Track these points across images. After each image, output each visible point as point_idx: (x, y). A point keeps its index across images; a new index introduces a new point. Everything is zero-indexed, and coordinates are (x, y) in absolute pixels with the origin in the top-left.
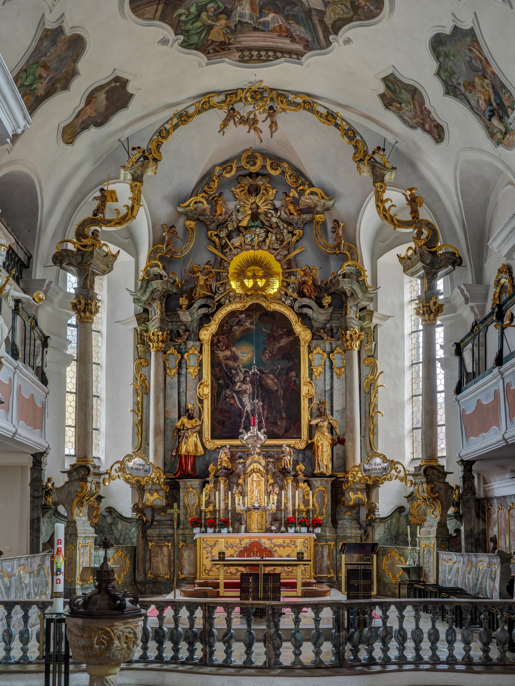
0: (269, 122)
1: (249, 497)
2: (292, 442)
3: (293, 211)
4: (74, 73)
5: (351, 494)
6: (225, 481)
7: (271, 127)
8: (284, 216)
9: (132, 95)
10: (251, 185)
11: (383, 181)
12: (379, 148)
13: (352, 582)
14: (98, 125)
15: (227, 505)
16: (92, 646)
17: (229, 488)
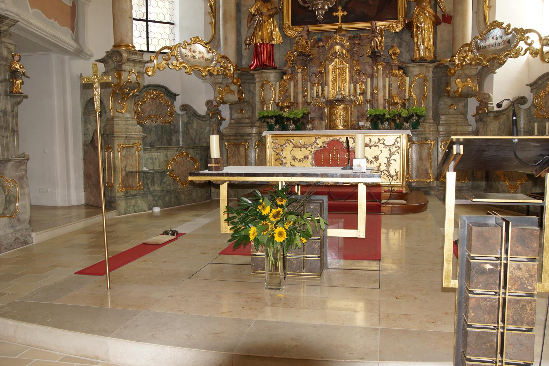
6: (303, 70)
17: (308, 78)
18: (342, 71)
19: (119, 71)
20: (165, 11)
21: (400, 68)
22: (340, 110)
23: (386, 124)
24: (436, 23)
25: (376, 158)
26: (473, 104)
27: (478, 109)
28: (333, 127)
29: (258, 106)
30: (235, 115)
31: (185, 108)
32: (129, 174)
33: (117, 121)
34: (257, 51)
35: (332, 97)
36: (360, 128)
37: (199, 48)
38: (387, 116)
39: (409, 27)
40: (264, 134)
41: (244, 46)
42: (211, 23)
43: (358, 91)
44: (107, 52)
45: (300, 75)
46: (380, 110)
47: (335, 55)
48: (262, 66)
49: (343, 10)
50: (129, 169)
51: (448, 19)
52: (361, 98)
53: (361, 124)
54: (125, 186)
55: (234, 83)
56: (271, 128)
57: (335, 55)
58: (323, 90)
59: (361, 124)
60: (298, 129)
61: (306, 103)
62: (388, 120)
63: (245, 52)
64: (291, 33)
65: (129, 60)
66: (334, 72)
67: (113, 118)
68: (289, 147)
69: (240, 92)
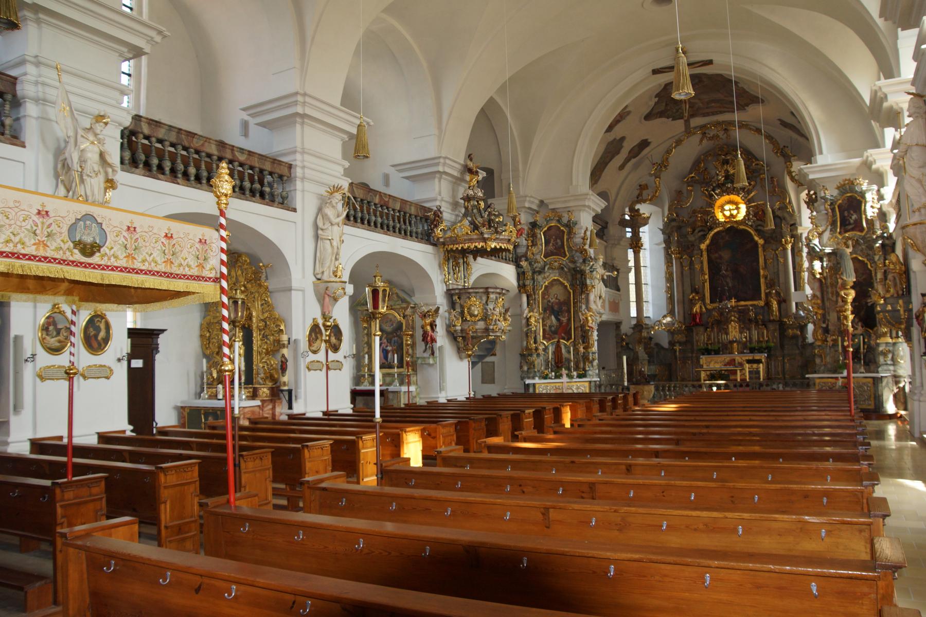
0: (725, 135)
2: (755, 303)
4: (622, 147)
5: (790, 330)
7: (727, 137)
11: (790, 162)
12: (784, 147)
13: (757, 375)
14: (634, 157)
18: (735, 328)
19: (640, 331)
21: (762, 325)
24: (779, 303)
26: (800, 340)
27: (802, 342)
29: (695, 343)
31: (657, 345)
34: (694, 316)
35: (731, 339)
36: (744, 353)
37: (669, 319)
39: (768, 304)
42: (669, 303)
43: (743, 337)
45: (715, 330)
46: (753, 345)
47: (732, 321)
48: (697, 325)
51: (785, 301)
52: (744, 339)
53: (745, 351)
56: (703, 354)
57: (732, 321)
59: (745, 351)
60: (715, 354)
61: (719, 342)
62: (757, 350)
64: (709, 307)
66: (732, 328)
67: (637, 352)
68: (713, 363)
69: (686, 337)
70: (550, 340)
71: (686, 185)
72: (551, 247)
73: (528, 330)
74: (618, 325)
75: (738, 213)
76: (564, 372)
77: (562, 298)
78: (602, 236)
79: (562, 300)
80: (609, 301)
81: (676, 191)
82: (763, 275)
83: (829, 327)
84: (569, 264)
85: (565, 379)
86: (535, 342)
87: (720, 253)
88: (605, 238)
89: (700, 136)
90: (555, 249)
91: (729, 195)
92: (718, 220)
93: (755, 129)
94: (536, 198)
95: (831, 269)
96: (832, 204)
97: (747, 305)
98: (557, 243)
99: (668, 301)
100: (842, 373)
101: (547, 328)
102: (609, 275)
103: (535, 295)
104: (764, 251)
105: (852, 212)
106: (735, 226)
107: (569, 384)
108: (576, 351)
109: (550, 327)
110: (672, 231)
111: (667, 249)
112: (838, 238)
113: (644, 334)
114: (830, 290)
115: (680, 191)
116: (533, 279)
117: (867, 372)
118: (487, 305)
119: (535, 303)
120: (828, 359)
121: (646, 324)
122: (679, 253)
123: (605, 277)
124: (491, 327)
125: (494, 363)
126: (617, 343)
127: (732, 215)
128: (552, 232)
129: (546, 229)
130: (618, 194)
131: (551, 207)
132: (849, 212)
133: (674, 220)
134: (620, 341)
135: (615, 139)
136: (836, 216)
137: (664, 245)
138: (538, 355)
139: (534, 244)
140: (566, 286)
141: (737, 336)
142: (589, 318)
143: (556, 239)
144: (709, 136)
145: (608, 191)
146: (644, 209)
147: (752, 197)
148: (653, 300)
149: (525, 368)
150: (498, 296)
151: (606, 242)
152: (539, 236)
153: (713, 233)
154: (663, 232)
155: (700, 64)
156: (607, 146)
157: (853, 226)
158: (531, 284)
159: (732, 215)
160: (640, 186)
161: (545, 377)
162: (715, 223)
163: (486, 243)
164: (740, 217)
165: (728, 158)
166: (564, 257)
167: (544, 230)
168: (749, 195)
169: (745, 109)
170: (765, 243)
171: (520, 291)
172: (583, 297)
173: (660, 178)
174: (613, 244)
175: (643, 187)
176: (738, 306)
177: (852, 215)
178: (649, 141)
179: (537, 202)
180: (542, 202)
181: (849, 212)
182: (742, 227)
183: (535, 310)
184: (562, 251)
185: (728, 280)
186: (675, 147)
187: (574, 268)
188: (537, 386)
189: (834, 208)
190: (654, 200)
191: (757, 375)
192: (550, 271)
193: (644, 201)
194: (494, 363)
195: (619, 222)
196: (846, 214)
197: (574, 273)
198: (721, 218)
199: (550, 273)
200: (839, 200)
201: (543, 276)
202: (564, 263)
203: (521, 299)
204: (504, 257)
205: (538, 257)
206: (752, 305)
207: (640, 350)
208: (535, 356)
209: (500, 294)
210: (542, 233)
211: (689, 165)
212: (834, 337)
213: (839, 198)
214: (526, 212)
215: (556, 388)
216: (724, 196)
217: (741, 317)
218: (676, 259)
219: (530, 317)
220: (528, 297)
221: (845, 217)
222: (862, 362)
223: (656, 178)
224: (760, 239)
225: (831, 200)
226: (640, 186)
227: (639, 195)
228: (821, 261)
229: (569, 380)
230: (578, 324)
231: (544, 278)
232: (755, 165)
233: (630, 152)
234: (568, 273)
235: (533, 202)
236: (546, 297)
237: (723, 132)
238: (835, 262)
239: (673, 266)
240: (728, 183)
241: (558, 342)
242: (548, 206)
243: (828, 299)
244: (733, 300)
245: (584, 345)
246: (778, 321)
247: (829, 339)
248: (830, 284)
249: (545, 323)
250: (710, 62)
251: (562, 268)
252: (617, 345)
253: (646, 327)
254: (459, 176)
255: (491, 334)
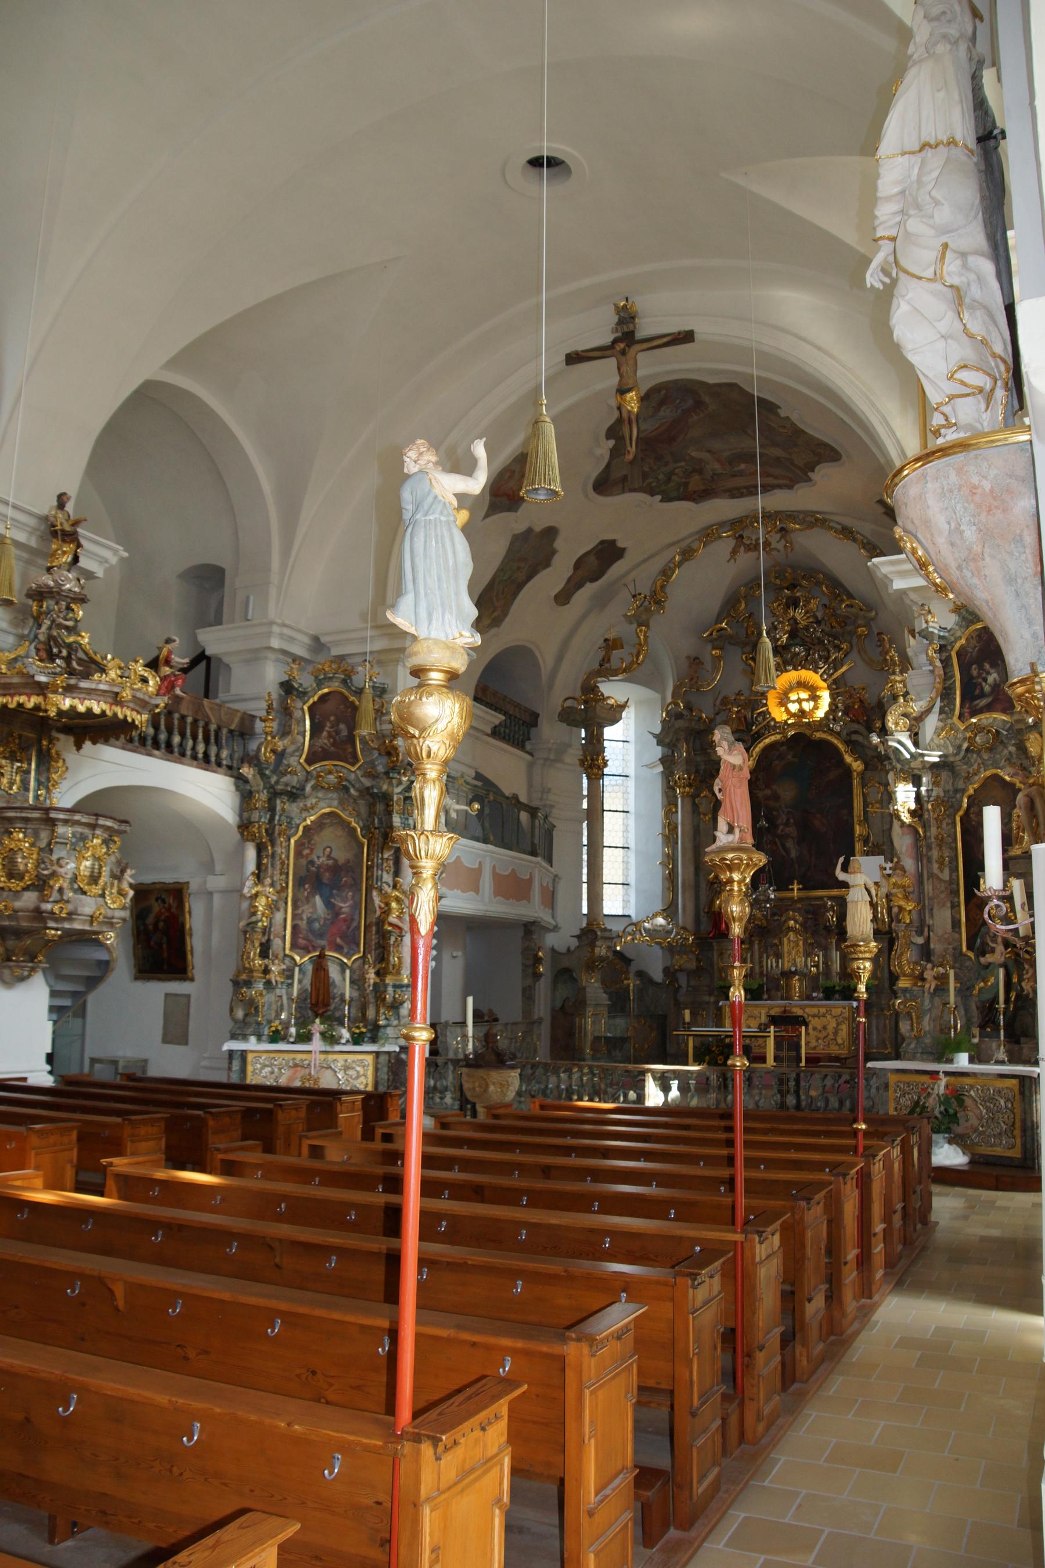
0: (783, 542)
1: (786, 959)
3: (834, 624)
4: (554, 552)
6: (760, 941)
8: (827, 629)
9: (624, 550)
10: (788, 598)
14: (593, 580)
15: (761, 967)
16: (474, 1089)
19: (592, 945)
20: (620, 872)
22: (795, 981)
23: (837, 996)
25: (825, 1028)
28: (788, 998)
30: (693, 983)
31: (641, 974)
32: (597, 1039)
33: (588, 990)
36: (813, 999)
37: (660, 921)
38: (837, 988)
40: (721, 1004)
41: (702, 914)
42: (669, 889)
44: (582, 930)
45: (756, 947)
46: (829, 984)
47: (790, 929)
49: (798, 884)
50: (597, 1034)
53: (814, 995)
54: (592, 1049)
55: (691, 952)
58: (777, 962)
59: (814, 995)
61: (761, 973)
63: (704, 919)
65: (602, 938)
67: (584, 988)
69: (698, 960)
70: (309, 952)
71: (709, 647)
72: (324, 740)
73: (248, 924)
74: (530, 929)
75: (816, 708)
76: (317, 1026)
77: (341, 855)
78: (523, 742)
79: (341, 861)
80: (495, 875)
81: (688, 657)
82: (860, 835)
83: (932, 946)
84: (362, 779)
85: (317, 1044)
86: (264, 954)
87: (774, 787)
88: (528, 746)
89: (732, 543)
90: (334, 744)
91: (796, 669)
92: (774, 719)
93: (839, 527)
94: (300, 631)
95: (939, 802)
96: (942, 649)
97: (821, 898)
98: (338, 732)
99: (667, 885)
100: (950, 1061)
101: (303, 924)
102: (466, 811)
103: (273, 845)
104: (864, 785)
105: (987, 666)
106: (808, 732)
107: (323, 1057)
108: (358, 982)
109: (310, 921)
110: (678, 740)
111: (668, 774)
112: (957, 730)
113: (601, 950)
114: (935, 854)
115: (696, 658)
116: (272, 810)
117: (1013, 1060)
118: (51, 851)
119: (273, 865)
120: (926, 1024)
121: (605, 930)
122: (690, 785)
123: (454, 815)
124: (47, 907)
125: (188, 996)
126: (525, 966)
127: (802, 711)
128: (330, 706)
129: (316, 698)
130: (560, 658)
131: (335, 652)
132: (981, 667)
133: (679, 716)
134: (531, 962)
135: (530, 530)
136: (953, 676)
137: (660, 769)
138: (268, 984)
139: (285, 732)
140: (354, 830)
141: (800, 961)
142: (394, 905)
143: (338, 725)
144: (748, 542)
145: (533, 648)
146: (613, 690)
147: (843, 673)
148: (637, 880)
149: (240, 1014)
150: (87, 831)
151: (531, 754)
152: (297, 714)
153: (761, 745)
154: (660, 740)
155: (665, 340)
156: (512, 543)
157: (990, 699)
158: (265, 819)
159: (802, 711)
160: (606, 640)
161: (276, 1037)
162: (767, 727)
163: (45, 697)
164: (820, 714)
165: (798, 594)
166: (353, 764)
167: (311, 701)
168: (836, 670)
169: (810, 480)
170: (866, 769)
171: (242, 834)
172: (386, 856)
173: (648, 626)
174: (546, 759)
175: (611, 645)
176: (809, 898)
177: (988, 673)
178: (620, 544)
179: (306, 640)
180: (316, 639)
181: (981, 667)
182: (819, 735)
183: (268, 881)
184: (350, 750)
185: (790, 844)
186: (680, 565)
187: (368, 788)
188: (250, 1057)
189: (949, 657)
190: (629, 672)
191: (794, 1053)
192: (320, 795)
193: (615, 673)
194: (188, 996)
195: (560, 714)
196: (974, 672)
197: (371, 800)
198: (779, 714)
199: (320, 799)
200: (960, 638)
201: (301, 805)
202: (352, 777)
203: (240, 853)
204: (200, 756)
205: (293, 761)
206: (830, 898)
207: (593, 986)
208: (260, 986)
209: (93, 827)
210: (306, 708)
211: (715, 605)
212: (941, 970)
213: (959, 634)
214: (277, 660)
215: (296, 1065)
216: (787, 671)
217: (809, 923)
218: (683, 797)
219: (256, 895)
220: (260, 849)
221: (972, 678)
222: (1002, 1032)
223: (640, 625)
224: (856, 760)
225: (940, 637)
226: (606, 640)
227: (603, 660)
228: (917, 782)
229: (328, 1048)
230: (373, 919)
231: (306, 809)
232: (847, 606)
233: (578, 565)
234: (361, 802)
235: (291, 640)
236: (306, 852)
237: (779, 535)
238: (950, 787)
239: (677, 812)
240: (795, 645)
241: (322, 956)
242: (329, 649)
243: (931, 875)
244: (796, 887)
245: (378, 966)
246: (886, 933)
247: (928, 975)
248: (936, 838)
249: (299, 911)
250: (686, 337)
251: (346, 789)
252: (523, 971)
253: (607, 934)
254: (33, 543)
255: (51, 924)
